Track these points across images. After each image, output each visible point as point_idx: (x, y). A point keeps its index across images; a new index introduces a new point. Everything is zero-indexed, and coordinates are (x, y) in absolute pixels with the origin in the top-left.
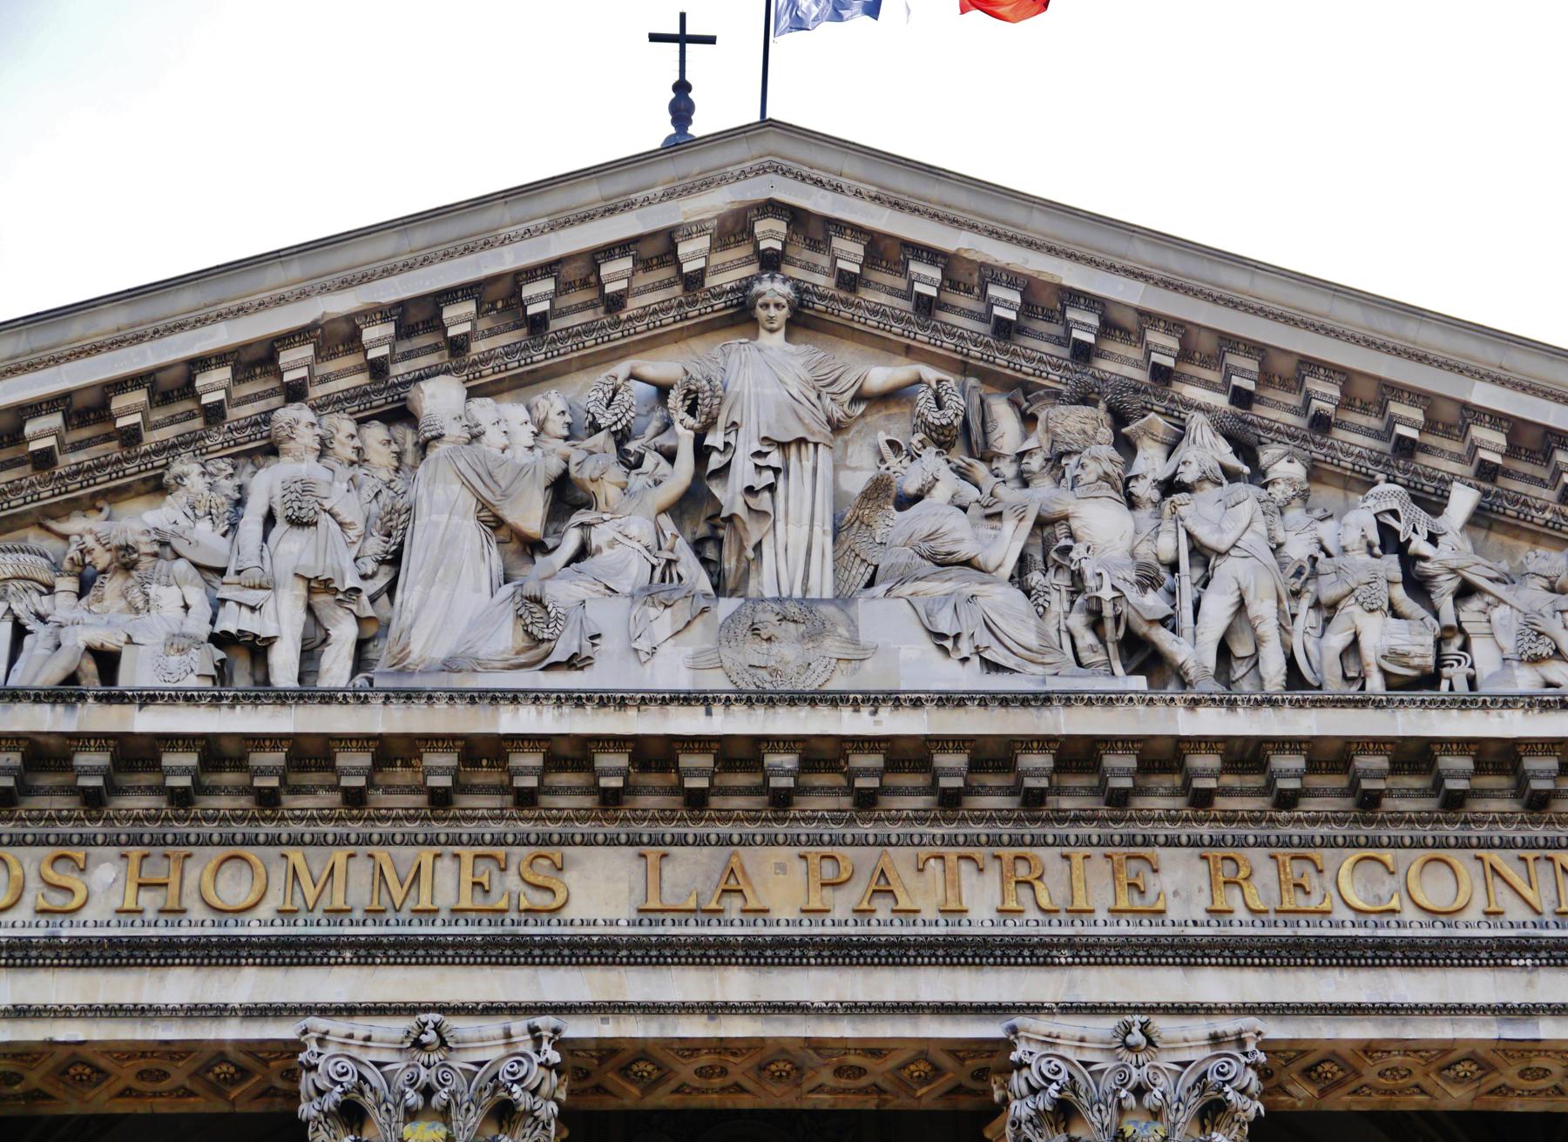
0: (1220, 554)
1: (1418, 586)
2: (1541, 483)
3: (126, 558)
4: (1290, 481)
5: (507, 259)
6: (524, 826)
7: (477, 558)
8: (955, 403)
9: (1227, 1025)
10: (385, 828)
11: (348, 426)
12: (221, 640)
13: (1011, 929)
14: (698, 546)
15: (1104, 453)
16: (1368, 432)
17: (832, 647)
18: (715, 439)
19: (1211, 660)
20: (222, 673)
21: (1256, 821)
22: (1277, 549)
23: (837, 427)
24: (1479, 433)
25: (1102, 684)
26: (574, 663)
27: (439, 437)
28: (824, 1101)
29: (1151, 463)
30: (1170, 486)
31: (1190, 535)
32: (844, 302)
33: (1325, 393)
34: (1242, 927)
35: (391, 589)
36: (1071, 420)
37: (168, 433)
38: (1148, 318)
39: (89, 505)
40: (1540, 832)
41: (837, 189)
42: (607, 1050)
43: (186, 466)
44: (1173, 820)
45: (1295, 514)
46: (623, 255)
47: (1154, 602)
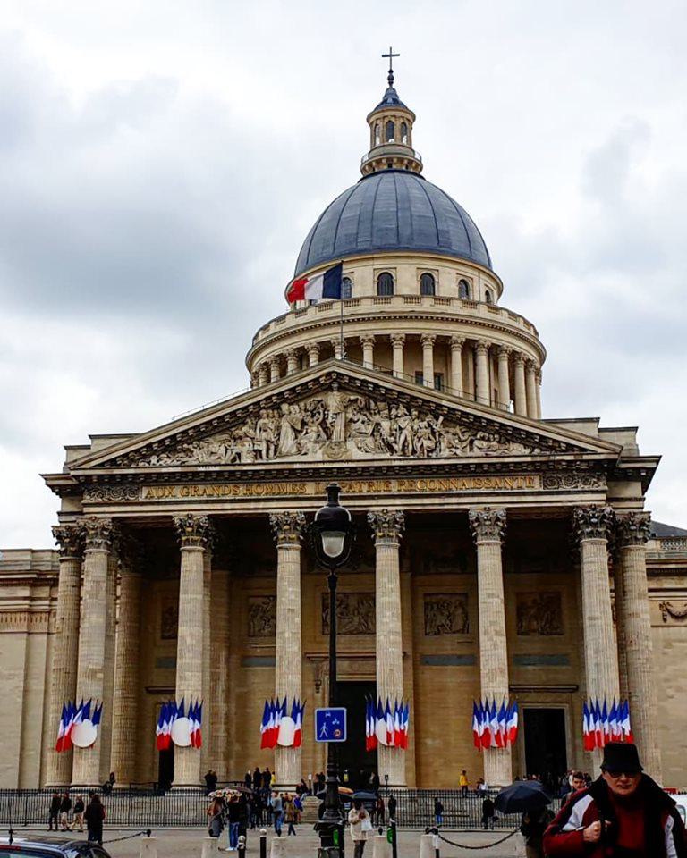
1: (433, 433)
3: (240, 438)
5: (293, 385)
7: (291, 434)
8: (364, 403)
9: (399, 508)
11: (270, 411)
12: (255, 451)
13: (369, 494)
14: (324, 429)
15: (387, 412)
17: (343, 450)
19: (401, 447)
20: (256, 457)
22: (412, 428)
23: (345, 407)
24: (444, 408)
25: (383, 457)
26: (305, 454)
29: (394, 412)
30: (396, 416)
33: (420, 402)
35: (279, 439)
36: (381, 405)
39: (234, 426)
43: (248, 420)
45: (416, 421)
47: (392, 439)
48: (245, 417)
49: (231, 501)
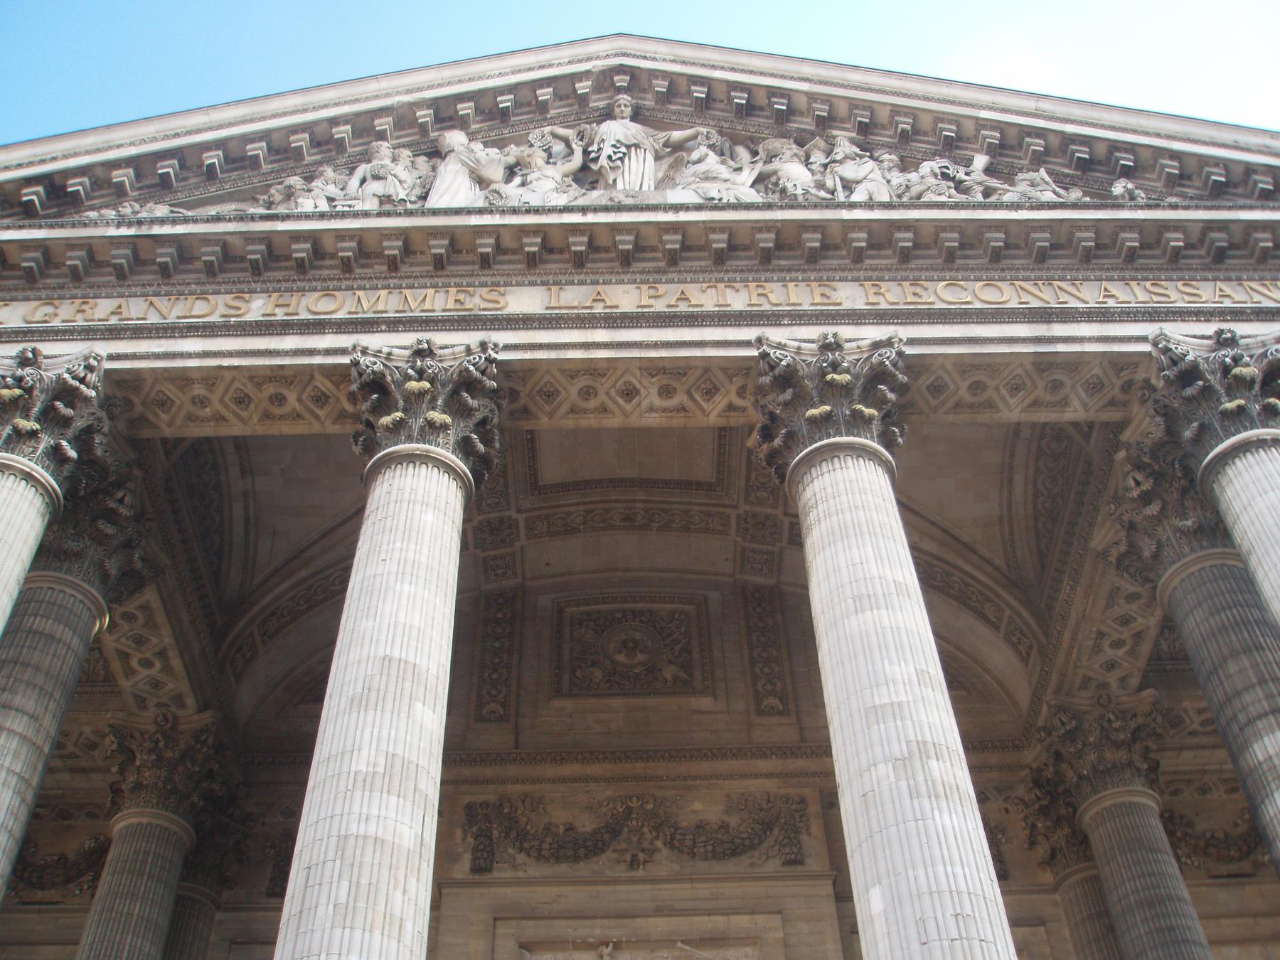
0: (858, 182)
2: (1020, 158)
4: (890, 160)
6: (483, 279)
10: (411, 281)
16: (928, 143)
18: (595, 147)
21: (889, 270)
22: (888, 182)
27: (452, 151)
28: (654, 420)
29: (818, 158)
31: (842, 179)
32: (660, 111)
34: (884, 306)
36: (775, 144)
37: (318, 157)
38: (811, 97)
40: (1044, 274)
41: (654, 59)
42: (530, 368)
44: (843, 270)
46: (548, 86)
48: (320, 163)
49: (210, 330)
